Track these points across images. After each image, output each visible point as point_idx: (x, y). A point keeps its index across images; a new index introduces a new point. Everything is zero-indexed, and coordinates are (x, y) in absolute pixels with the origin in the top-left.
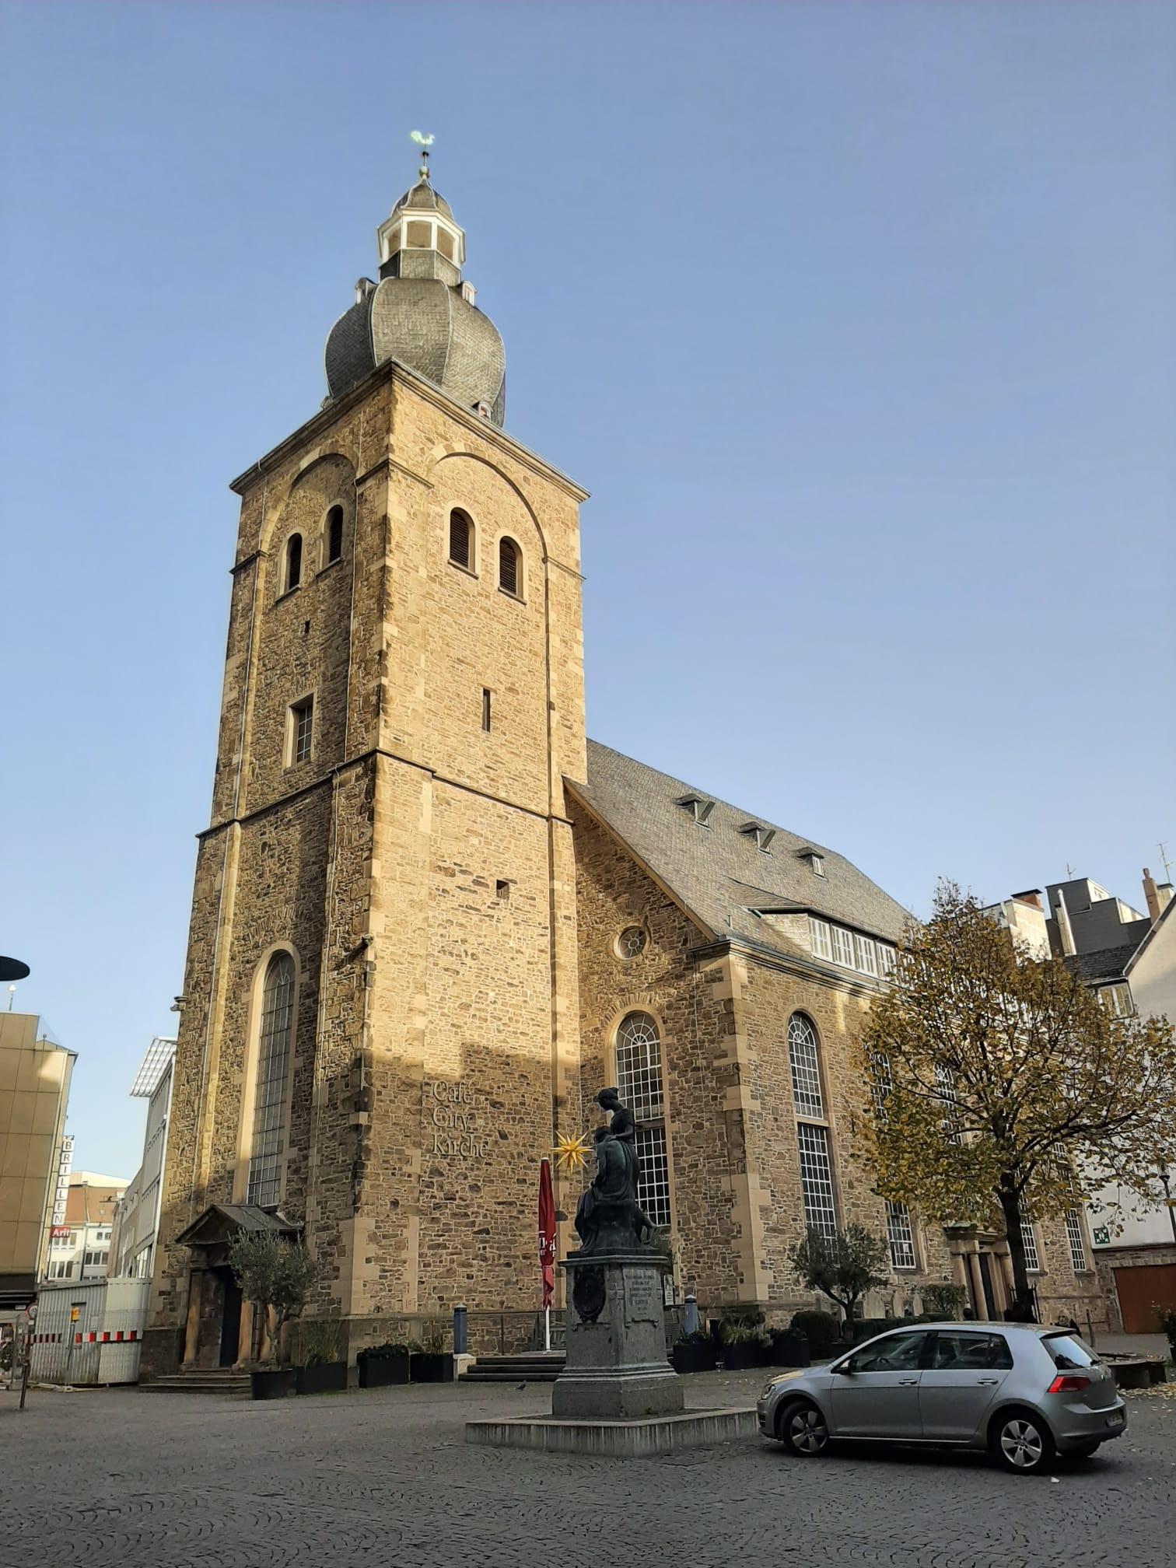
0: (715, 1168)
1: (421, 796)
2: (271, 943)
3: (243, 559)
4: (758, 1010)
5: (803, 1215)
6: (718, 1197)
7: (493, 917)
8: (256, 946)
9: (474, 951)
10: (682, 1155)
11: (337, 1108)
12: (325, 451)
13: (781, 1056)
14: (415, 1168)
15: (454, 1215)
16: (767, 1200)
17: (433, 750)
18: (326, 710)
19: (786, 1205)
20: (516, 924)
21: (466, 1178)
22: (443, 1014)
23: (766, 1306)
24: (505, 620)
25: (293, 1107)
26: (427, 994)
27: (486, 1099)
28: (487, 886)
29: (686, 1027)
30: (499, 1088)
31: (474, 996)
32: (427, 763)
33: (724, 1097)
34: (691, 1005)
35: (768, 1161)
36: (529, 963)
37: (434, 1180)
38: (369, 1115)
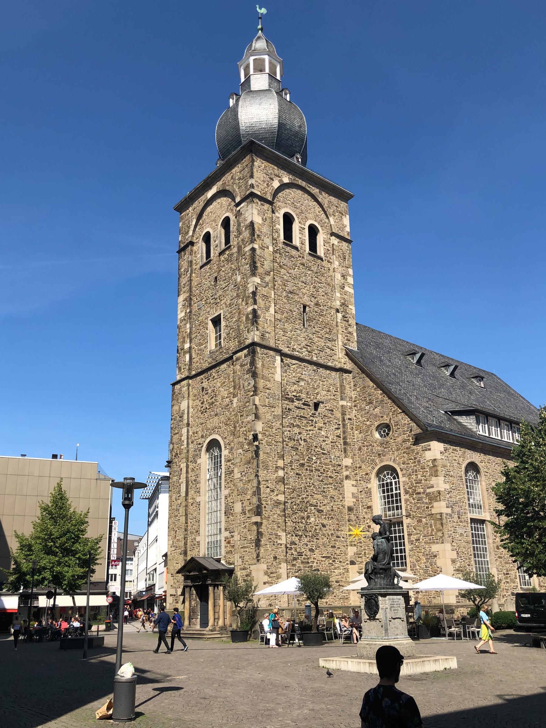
0: (428, 541)
1: (275, 364)
3: (182, 245)
4: (449, 464)
5: (473, 563)
6: (430, 555)
7: (313, 421)
9: (305, 438)
10: (411, 535)
11: (246, 514)
12: (219, 188)
13: (461, 486)
14: (283, 541)
15: (302, 562)
16: (454, 555)
17: (280, 340)
18: (228, 322)
19: (464, 558)
20: (324, 423)
21: (307, 546)
22: (292, 469)
23: (455, 606)
24: (312, 268)
25: (225, 513)
26: (284, 460)
27: (315, 509)
28: (309, 406)
29: (412, 473)
30: (320, 503)
31: (306, 459)
32: (277, 346)
33: (432, 507)
34: (415, 462)
35: (455, 538)
36: (332, 442)
37: (292, 547)
38: (261, 518)
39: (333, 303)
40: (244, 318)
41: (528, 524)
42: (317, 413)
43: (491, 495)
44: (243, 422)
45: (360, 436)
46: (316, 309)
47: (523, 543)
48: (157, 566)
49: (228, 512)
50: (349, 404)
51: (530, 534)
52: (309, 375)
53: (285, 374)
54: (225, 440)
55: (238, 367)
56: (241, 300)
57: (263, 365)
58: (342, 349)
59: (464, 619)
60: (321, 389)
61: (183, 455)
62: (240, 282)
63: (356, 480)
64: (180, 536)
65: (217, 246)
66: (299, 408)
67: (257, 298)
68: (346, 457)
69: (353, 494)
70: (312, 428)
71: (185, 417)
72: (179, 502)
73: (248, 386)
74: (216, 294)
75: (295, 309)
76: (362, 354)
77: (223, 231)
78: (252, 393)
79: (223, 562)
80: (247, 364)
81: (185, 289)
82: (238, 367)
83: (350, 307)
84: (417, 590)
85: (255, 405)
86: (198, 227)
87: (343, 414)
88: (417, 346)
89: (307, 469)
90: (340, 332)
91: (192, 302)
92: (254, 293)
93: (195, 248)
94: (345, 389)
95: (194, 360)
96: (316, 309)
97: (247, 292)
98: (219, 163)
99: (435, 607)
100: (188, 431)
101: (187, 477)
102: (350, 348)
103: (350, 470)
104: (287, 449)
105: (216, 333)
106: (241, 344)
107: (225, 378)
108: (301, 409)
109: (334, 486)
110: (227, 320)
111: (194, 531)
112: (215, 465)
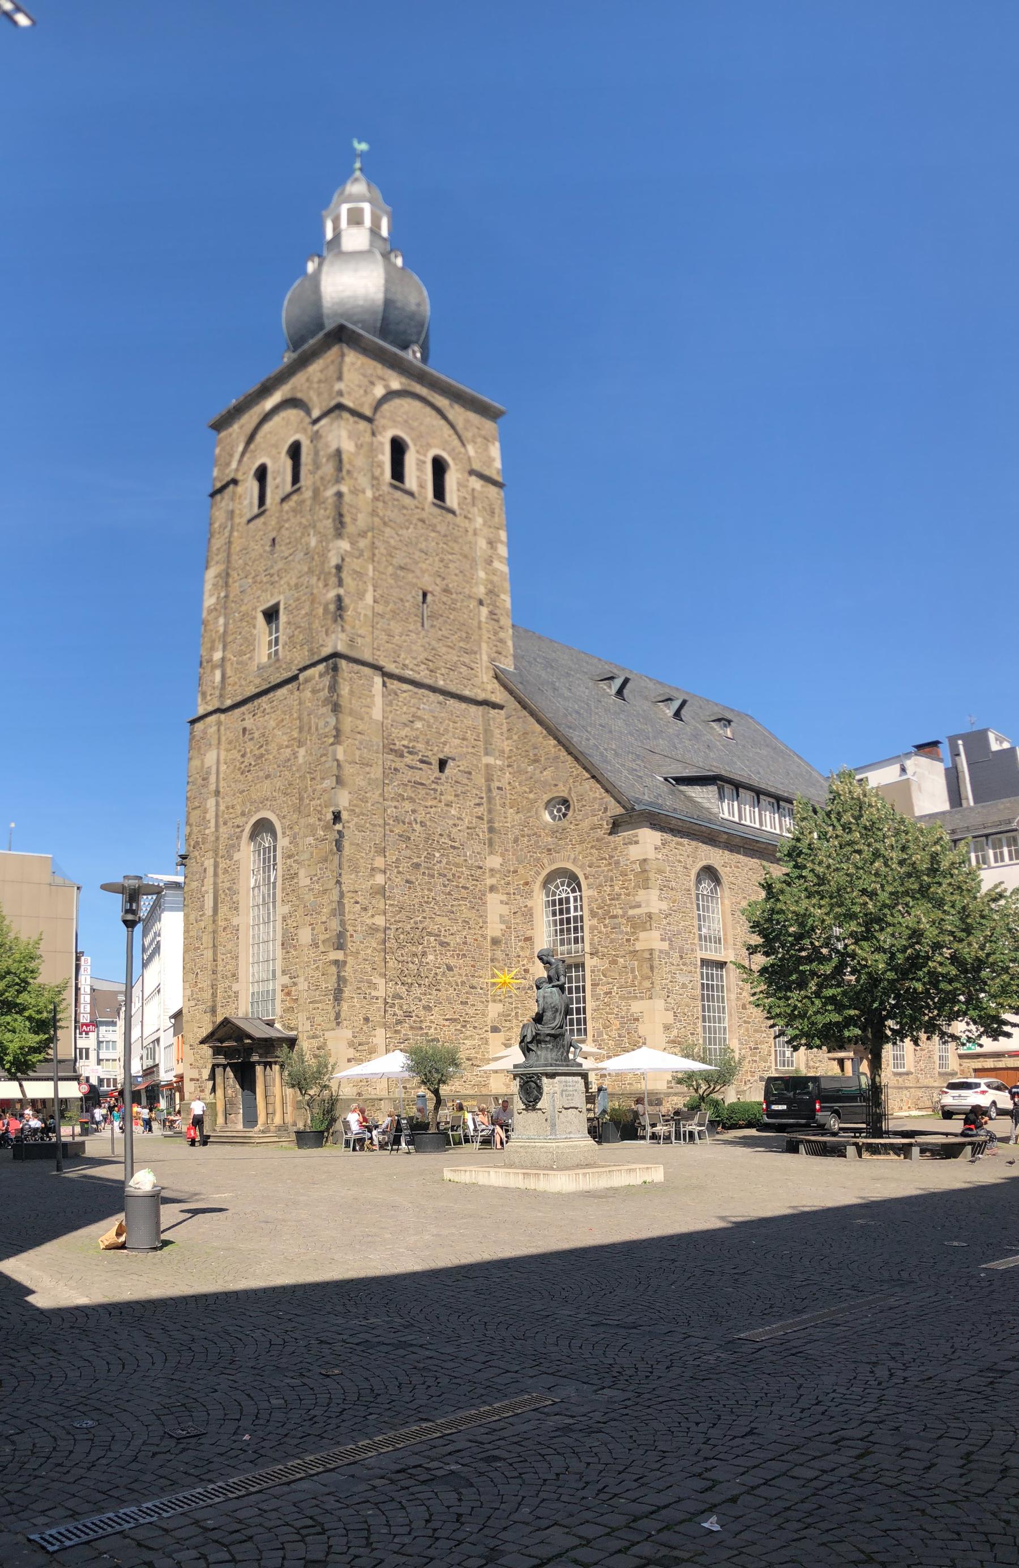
1: (373, 690)
2: (255, 812)
8: (243, 814)
14: (381, 993)
20: (456, 796)
25: (283, 944)
26: (385, 857)
28: (430, 764)
36: (468, 828)
39: (475, 590)
40: (321, 611)
41: (801, 968)
42: (443, 776)
43: (738, 922)
44: (315, 790)
45: (517, 817)
46: (445, 599)
47: (788, 998)
48: (161, 1034)
49: (288, 943)
50: (499, 763)
51: (802, 985)
52: (431, 711)
53: (388, 709)
54: (284, 821)
55: (308, 694)
56: (315, 578)
57: (352, 692)
58: (487, 668)
59: (677, 1113)
60: (451, 734)
61: (209, 846)
62: (316, 547)
63: (507, 894)
64: (205, 982)
65: (277, 487)
66: (412, 768)
67: (344, 575)
68: (491, 853)
69: (501, 916)
70: (434, 803)
71: (213, 779)
72: (202, 924)
73: (325, 726)
74: (272, 567)
75: (409, 597)
76: (521, 676)
77: (289, 463)
78: (331, 740)
79: (277, 1025)
80: (323, 689)
81: (220, 557)
82: (308, 694)
83: (503, 596)
84: (604, 1072)
85: (337, 760)
86: (247, 455)
87: (489, 779)
88: (616, 666)
89: (424, 873)
90: (485, 638)
91: (231, 580)
92: (339, 568)
93: (240, 489)
94: (492, 736)
95: (230, 681)
96: (445, 599)
97: (326, 565)
98: (288, 358)
99: (629, 1095)
100: (217, 804)
101: (215, 884)
102: (501, 666)
103: (498, 876)
104: (392, 838)
105: (271, 634)
106: (313, 654)
107: (284, 713)
108: (417, 768)
109: (470, 902)
110: (291, 612)
111: (229, 974)
112: (264, 863)
